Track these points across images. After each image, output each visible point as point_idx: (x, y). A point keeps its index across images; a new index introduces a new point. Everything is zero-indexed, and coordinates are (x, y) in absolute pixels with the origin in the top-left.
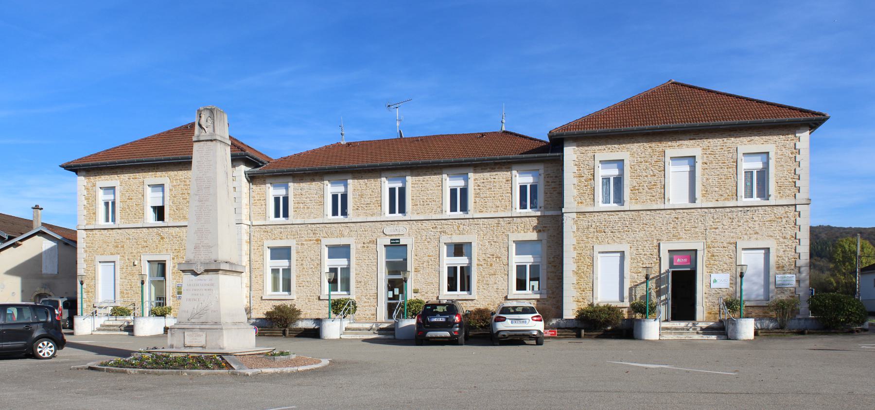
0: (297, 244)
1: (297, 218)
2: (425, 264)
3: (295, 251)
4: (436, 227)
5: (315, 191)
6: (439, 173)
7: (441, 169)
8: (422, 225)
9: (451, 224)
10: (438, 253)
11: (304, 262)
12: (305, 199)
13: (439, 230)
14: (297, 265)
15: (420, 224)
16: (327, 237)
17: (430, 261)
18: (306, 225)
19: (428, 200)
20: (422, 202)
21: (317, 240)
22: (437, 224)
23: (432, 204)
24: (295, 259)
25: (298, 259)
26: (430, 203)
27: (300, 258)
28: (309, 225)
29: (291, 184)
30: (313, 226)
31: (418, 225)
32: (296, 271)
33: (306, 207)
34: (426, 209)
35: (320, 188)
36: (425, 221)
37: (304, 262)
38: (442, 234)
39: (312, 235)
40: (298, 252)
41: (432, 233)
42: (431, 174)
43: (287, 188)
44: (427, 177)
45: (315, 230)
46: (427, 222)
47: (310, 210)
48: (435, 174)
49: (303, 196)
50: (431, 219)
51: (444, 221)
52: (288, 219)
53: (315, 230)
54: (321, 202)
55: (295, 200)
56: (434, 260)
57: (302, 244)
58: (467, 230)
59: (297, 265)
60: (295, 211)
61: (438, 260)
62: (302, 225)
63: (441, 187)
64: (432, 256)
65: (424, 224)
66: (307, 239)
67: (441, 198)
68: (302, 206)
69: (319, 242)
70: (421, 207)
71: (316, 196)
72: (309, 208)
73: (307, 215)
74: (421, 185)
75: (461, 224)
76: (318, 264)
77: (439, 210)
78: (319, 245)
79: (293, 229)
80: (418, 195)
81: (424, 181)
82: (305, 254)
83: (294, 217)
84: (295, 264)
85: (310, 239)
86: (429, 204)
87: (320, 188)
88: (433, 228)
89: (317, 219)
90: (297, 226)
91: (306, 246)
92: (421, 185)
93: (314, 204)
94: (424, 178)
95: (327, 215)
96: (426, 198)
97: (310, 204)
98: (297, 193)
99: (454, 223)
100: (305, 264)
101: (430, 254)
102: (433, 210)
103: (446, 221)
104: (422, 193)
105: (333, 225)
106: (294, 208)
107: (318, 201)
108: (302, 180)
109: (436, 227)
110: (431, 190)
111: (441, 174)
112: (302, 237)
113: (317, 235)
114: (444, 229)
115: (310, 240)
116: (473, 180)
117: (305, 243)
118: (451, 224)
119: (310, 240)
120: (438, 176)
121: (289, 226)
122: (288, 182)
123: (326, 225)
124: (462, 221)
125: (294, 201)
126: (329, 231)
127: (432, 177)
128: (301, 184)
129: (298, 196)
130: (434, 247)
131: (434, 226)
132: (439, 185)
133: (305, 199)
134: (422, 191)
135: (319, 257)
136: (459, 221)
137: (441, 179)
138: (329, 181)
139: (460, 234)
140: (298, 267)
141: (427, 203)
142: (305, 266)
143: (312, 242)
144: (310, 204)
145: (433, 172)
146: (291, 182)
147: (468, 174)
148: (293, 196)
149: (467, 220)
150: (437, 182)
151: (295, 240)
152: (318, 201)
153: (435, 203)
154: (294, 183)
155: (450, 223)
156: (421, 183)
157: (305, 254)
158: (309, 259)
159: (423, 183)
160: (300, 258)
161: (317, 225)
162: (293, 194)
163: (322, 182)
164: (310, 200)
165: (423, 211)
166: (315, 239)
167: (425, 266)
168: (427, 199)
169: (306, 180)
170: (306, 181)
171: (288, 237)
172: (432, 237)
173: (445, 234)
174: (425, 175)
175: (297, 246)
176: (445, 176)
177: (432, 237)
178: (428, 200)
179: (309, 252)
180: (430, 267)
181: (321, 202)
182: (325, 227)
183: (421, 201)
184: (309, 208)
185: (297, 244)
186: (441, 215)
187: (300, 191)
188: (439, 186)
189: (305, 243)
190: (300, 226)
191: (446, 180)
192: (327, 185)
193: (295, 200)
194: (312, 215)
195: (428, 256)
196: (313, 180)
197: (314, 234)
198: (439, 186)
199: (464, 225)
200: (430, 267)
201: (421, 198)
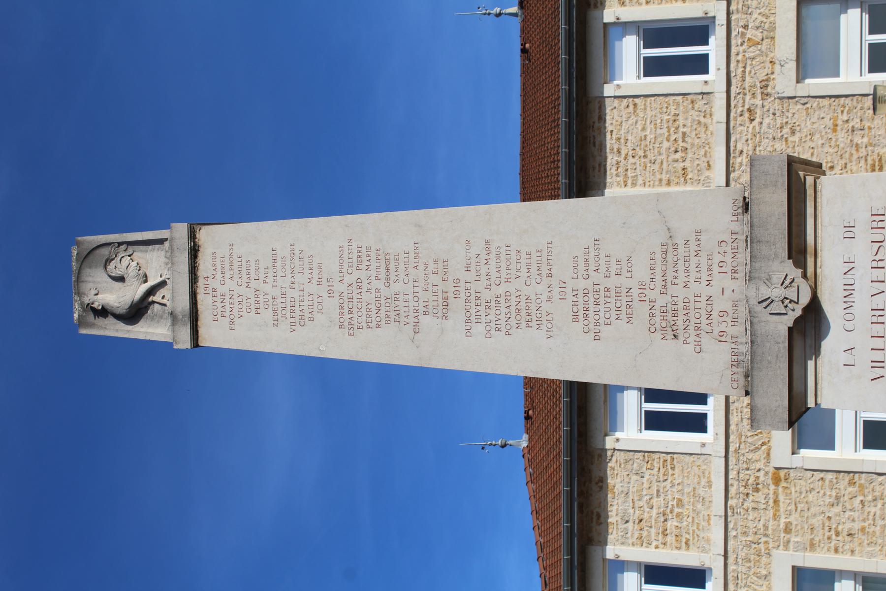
0: (786, 548)
1: (708, 541)
2: (857, 140)
3: (808, 554)
4: (749, 110)
5: (634, 478)
6: (600, 108)
7: (587, 103)
8: (741, 152)
9: (741, 65)
10: (826, 102)
11: (844, 528)
12: (655, 511)
13: (758, 101)
14: (852, 551)
15: (739, 160)
16: (769, 450)
17: (851, 124)
18: (730, 513)
19: (673, 137)
20: (678, 156)
21: (777, 481)
22: (740, 109)
23: (684, 126)
24: (832, 555)
25: (832, 545)
26: (681, 130)
27: (829, 538)
28: (730, 503)
29: (611, 552)
30: (733, 491)
31: (741, 164)
32: (871, 555)
33: (676, 510)
34: (697, 141)
35: (627, 462)
36: (732, 144)
37: (844, 528)
38: (769, 90)
39: (760, 497)
40: (812, 546)
41: (766, 121)
42: (602, 131)
43: (621, 566)
44: (610, 142)
45: (746, 486)
46: (733, 139)
47: (685, 499)
48: (602, 119)
49: (646, 516)
50: (724, 126)
51: (733, 89)
52: (711, 569)
53: (746, 486)
54: (665, 461)
55: (654, 543)
56: (848, 113)
57: (788, 530)
58: (760, 18)
59: (852, 551)
60: (687, 543)
61: (848, 101)
62: (731, 526)
63: (637, 100)
64: (836, 118)
65: (739, 147)
66: (770, 513)
67: (667, 99)
68: (672, 524)
69: (782, 473)
70: (690, 155)
71: (647, 477)
72: (680, 500)
73: (699, 506)
74: (631, 160)
75: (743, 35)
76: (852, 483)
77: (700, 104)
78: (792, 474)
79: (742, 554)
80: (656, 167)
81: (619, 152)
82: (817, 521)
83: (704, 551)
84: (848, 556)
85: (771, 502)
86: (684, 134)
87: (627, 462)
88: (752, 120)
89: (713, 478)
90: (731, 543)
91: (792, 519)
92: (631, 160)
93: (668, 484)
94: (612, 149)
95: (703, 445)
96: (666, 144)
97: (670, 497)
98: (636, 535)
99: (740, 57)
100: (848, 525)
101: (830, 124)
102: (699, 122)
103: (734, 81)
104: (651, 156)
105: (733, 427)
106: (679, 548)
107: (662, 471)
108: (599, 516)
109: (749, 110)
110: (644, 129)
111: (602, 99)
112: (766, 527)
113: (762, 479)
114: (755, 86)
115: (776, 502)
116: (624, 8)
117: (783, 520)
118: (741, 65)
119: (776, 502)
120: (608, 111)
121: (731, 567)
122: (604, 560)
123: (731, 449)
124: (734, 34)
125: (657, 547)
126: (750, 440)
127: (609, 128)
128: (610, 520)
129: (645, 534)
130: (808, 114)
131: (747, 115)
132: (631, 107)
133: (655, 511)
134: (645, 157)
135: (830, 476)
136: (733, 42)
137: (616, 101)
138: (606, 435)
139: (773, 38)
140: (857, 549)
141: (680, 140)
142: (857, 526)
143: (781, 498)
144: (670, 497)
145: (597, 125)
146: (604, 552)
147: (605, 24)
148: (643, 549)
149: (734, 17)
150: (624, 113)
151: (774, 552)
152: (662, 471)
153: (680, 118)
154: (606, 545)
155: (740, 70)
156: (625, 158)
157: (817, 521)
158: (837, 509)
159: (623, 152)
160: (829, 538)
161: (731, 476)
162: (637, 549)
163: (609, 453)
164: (658, 496)
165: (702, 152)
166: (772, 487)
167: (865, 140)
168: (668, 140)
169: (600, 506)
170: (603, 505)
171: (764, 572)
172: (779, 121)
173: (771, 83)
174: (602, 147)
175: (791, 545)
176: (609, 90)
177: (779, 121)
178: (673, 137)
179: (813, 510)
180: (867, 124)
181: (665, 461)
182: (737, 451)
183: (674, 156)
184: (680, 500)
185: (786, 548)
186: (717, 95)
187: (630, 524)
188: (635, 105)
189: (783, 520)
190: (732, 533)
191: (618, 86)
192: (618, 440)
193: (654, 543)
194: (701, 491)
195: (835, 131)
196: (602, 481)
197: (757, 490)
198: (635, 105)
199: (746, 27)
200: (867, 124)
201: (664, 157)
